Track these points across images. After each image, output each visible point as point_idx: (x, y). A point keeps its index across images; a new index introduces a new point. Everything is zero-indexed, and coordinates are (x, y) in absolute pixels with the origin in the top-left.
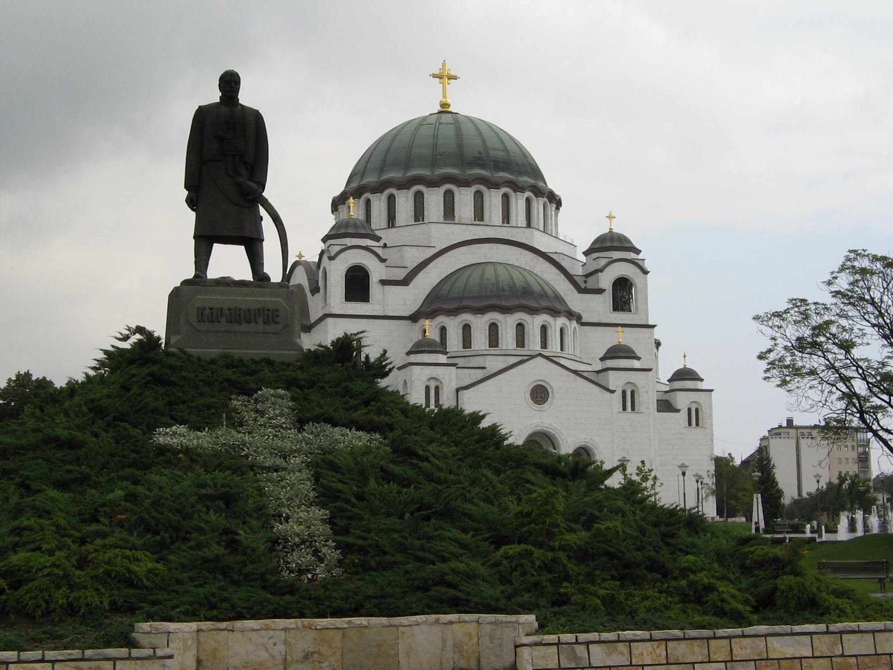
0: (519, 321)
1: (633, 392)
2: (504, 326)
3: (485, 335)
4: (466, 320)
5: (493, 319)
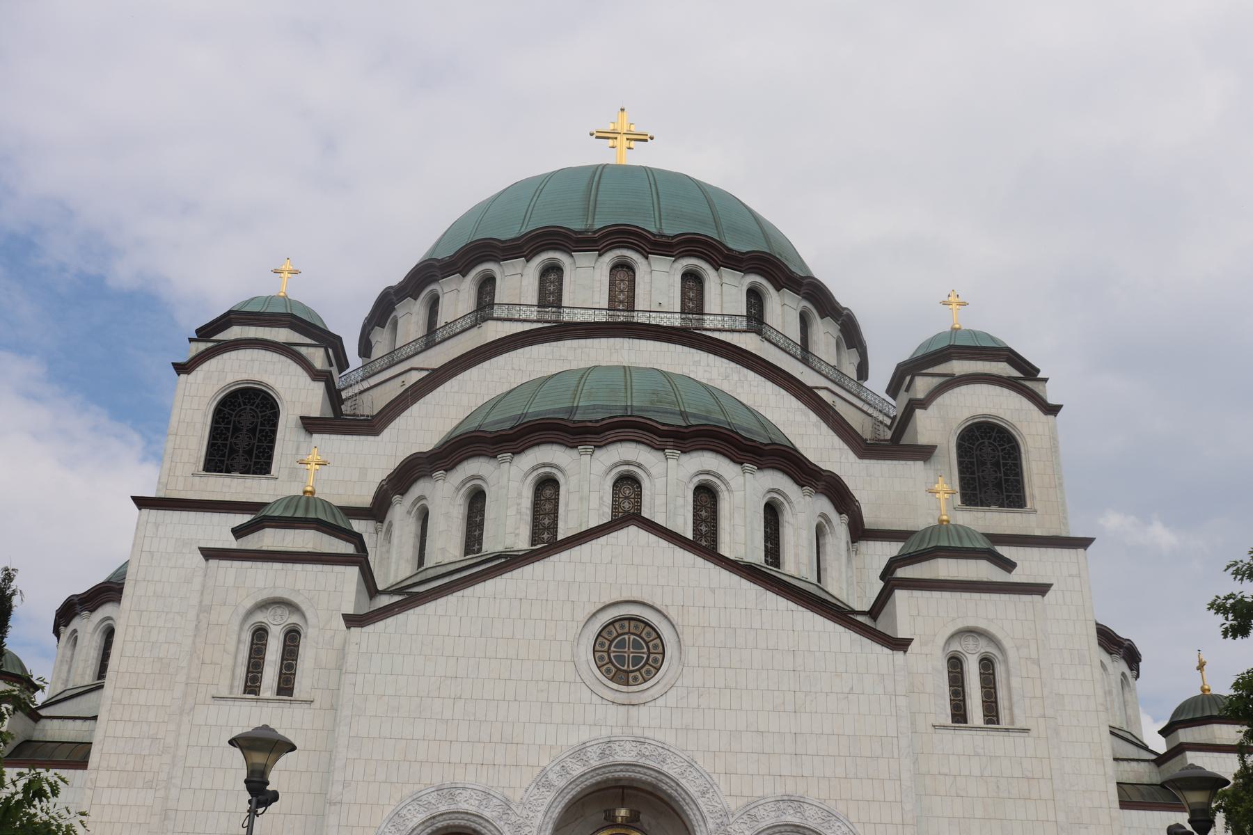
0: (626, 468)
1: (987, 664)
2: (573, 481)
3: (519, 512)
4: (474, 477)
5: (544, 465)
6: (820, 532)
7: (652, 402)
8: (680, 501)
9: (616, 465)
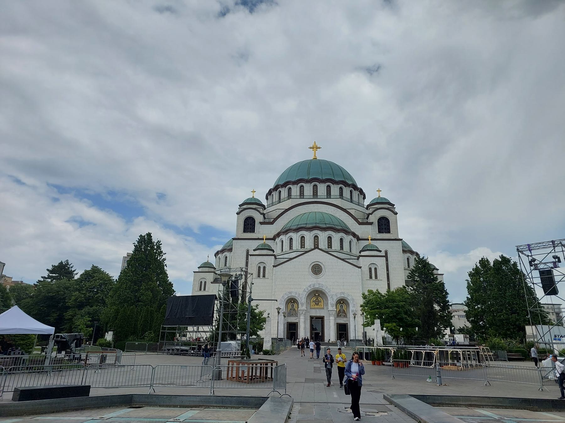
3: (299, 243)
4: (290, 236)
5: (302, 234)
6: (350, 242)
7: (320, 222)
8: (325, 240)
9: (314, 234)
